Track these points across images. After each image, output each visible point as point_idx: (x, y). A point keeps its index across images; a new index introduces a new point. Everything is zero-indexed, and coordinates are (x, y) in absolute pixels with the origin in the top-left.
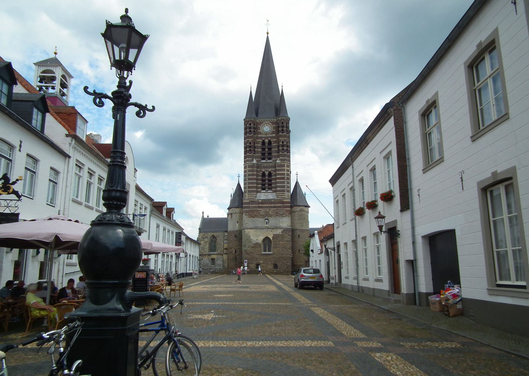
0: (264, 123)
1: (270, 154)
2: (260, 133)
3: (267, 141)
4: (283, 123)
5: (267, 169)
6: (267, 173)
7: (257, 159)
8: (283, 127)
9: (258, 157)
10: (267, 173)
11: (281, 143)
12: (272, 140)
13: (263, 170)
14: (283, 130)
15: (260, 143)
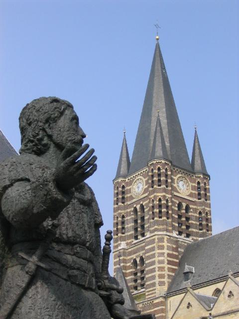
0: (136, 179)
1: (143, 227)
2: (132, 198)
3: (138, 207)
4: (159, 169)
5: (138, 254)
6: (138, 260)
7: (127, 241)
8: (166, 176)
9: (130, 237)
10: (138, 260)
11: (158, 202)
12: (144, 204)
13: (134, 256)
14: (159, 180)
15: (132, 213)
